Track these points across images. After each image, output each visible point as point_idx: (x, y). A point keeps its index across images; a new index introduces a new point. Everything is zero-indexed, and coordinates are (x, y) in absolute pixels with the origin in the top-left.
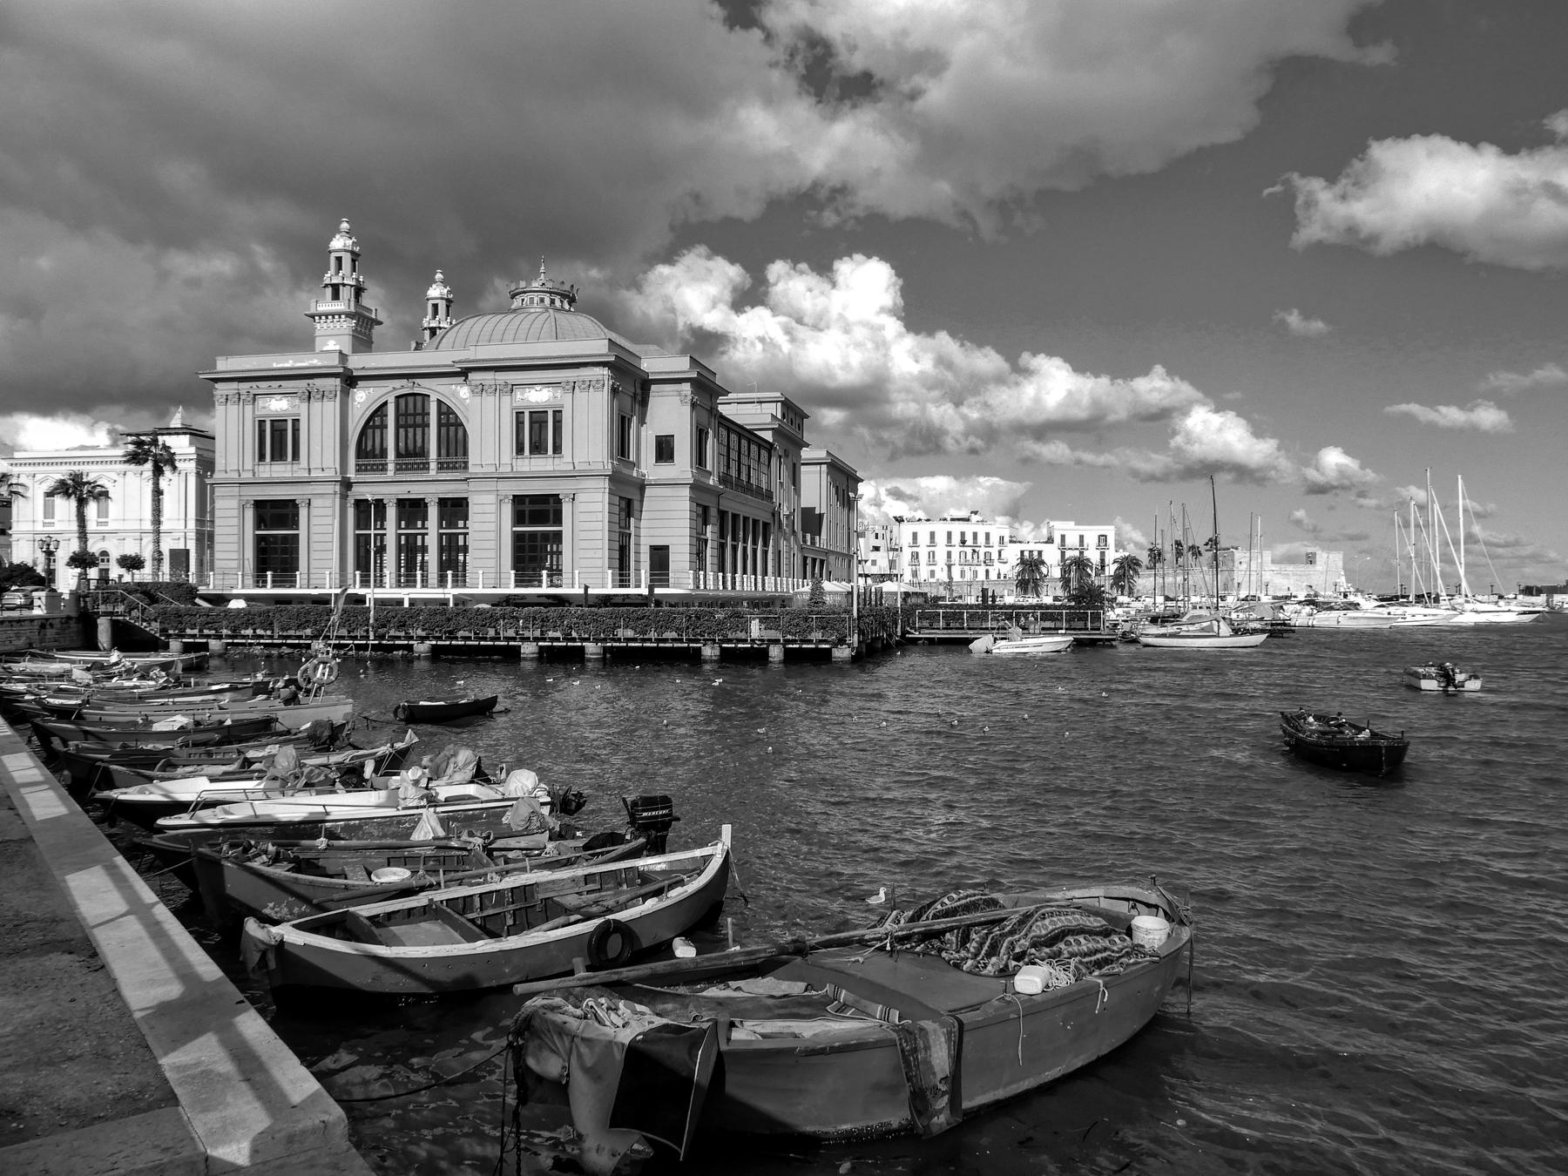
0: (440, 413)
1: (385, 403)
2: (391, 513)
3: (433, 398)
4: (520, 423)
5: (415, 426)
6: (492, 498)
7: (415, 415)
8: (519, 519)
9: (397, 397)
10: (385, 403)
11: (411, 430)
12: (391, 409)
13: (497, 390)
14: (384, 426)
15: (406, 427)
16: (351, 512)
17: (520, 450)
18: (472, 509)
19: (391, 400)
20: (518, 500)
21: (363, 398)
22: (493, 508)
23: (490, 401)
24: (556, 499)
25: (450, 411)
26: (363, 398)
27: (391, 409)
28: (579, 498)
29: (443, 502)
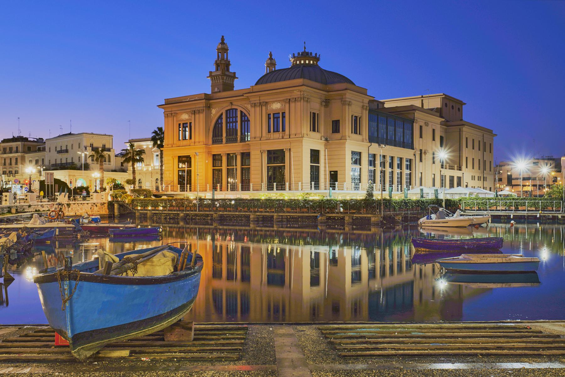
0: (242, 116)
1: (222, 114)
2: (224, 160)
3: (239, 109)
4: (269, 118)
5: (233, 122)
6: (259, 152)
7: (233, 117)
8: (270, 160)
9: (227, 111)
10: (222, 114)
11: (231, 124)
12: (224, 116)
13: (261, 105)
14: (222, 123)
15: (230, 123)
16: (211, 159)
17: (269, 132)
18: (252, 156)
19: (224, 111)
20: (269, 152)
21: (214, 111)
22: (260, 156)
23: (258, 109)
24: (282, 152)
25: (245, 115)
26: (215, 112)
27: (224, 116)
28: (292, 150)
29: (243, 154)
